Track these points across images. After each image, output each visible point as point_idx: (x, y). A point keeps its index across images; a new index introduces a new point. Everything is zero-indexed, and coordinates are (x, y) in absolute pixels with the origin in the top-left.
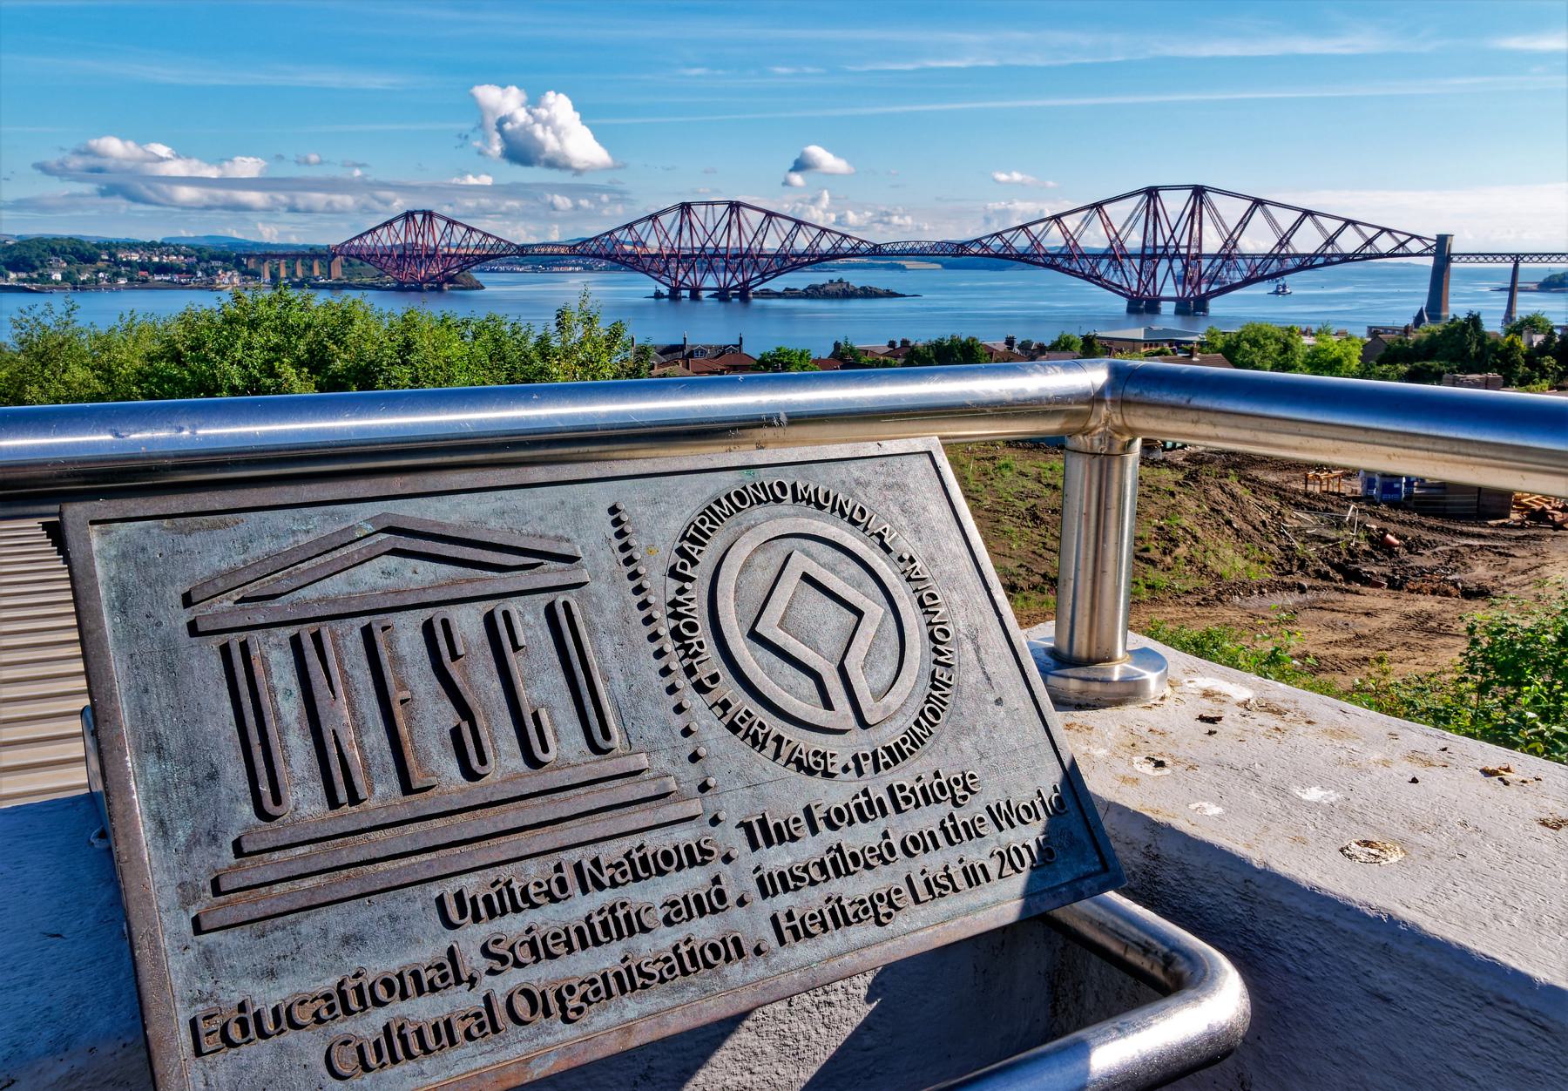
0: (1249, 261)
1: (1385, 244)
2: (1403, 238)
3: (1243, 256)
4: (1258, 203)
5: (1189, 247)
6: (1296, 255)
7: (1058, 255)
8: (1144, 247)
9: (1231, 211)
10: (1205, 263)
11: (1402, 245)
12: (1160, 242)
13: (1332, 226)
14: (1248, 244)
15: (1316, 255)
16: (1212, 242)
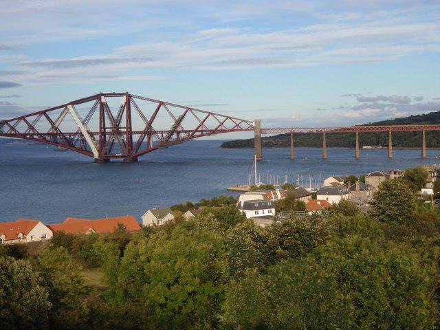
0: (160, 135)
1: (229, 124)
2: (238, 122)
3: (155, 132)
4: (161, 103)
5: (126, 128)
6: (185, 132)
7: (48, 134)
8: (101, 128)
9: (149, 109)
10: (136, 138)
11: (238, 125)
12: (108, 124)
13: (202, 116)
14: (156, 126)
15: (197, 130)
16: (138, 125)
